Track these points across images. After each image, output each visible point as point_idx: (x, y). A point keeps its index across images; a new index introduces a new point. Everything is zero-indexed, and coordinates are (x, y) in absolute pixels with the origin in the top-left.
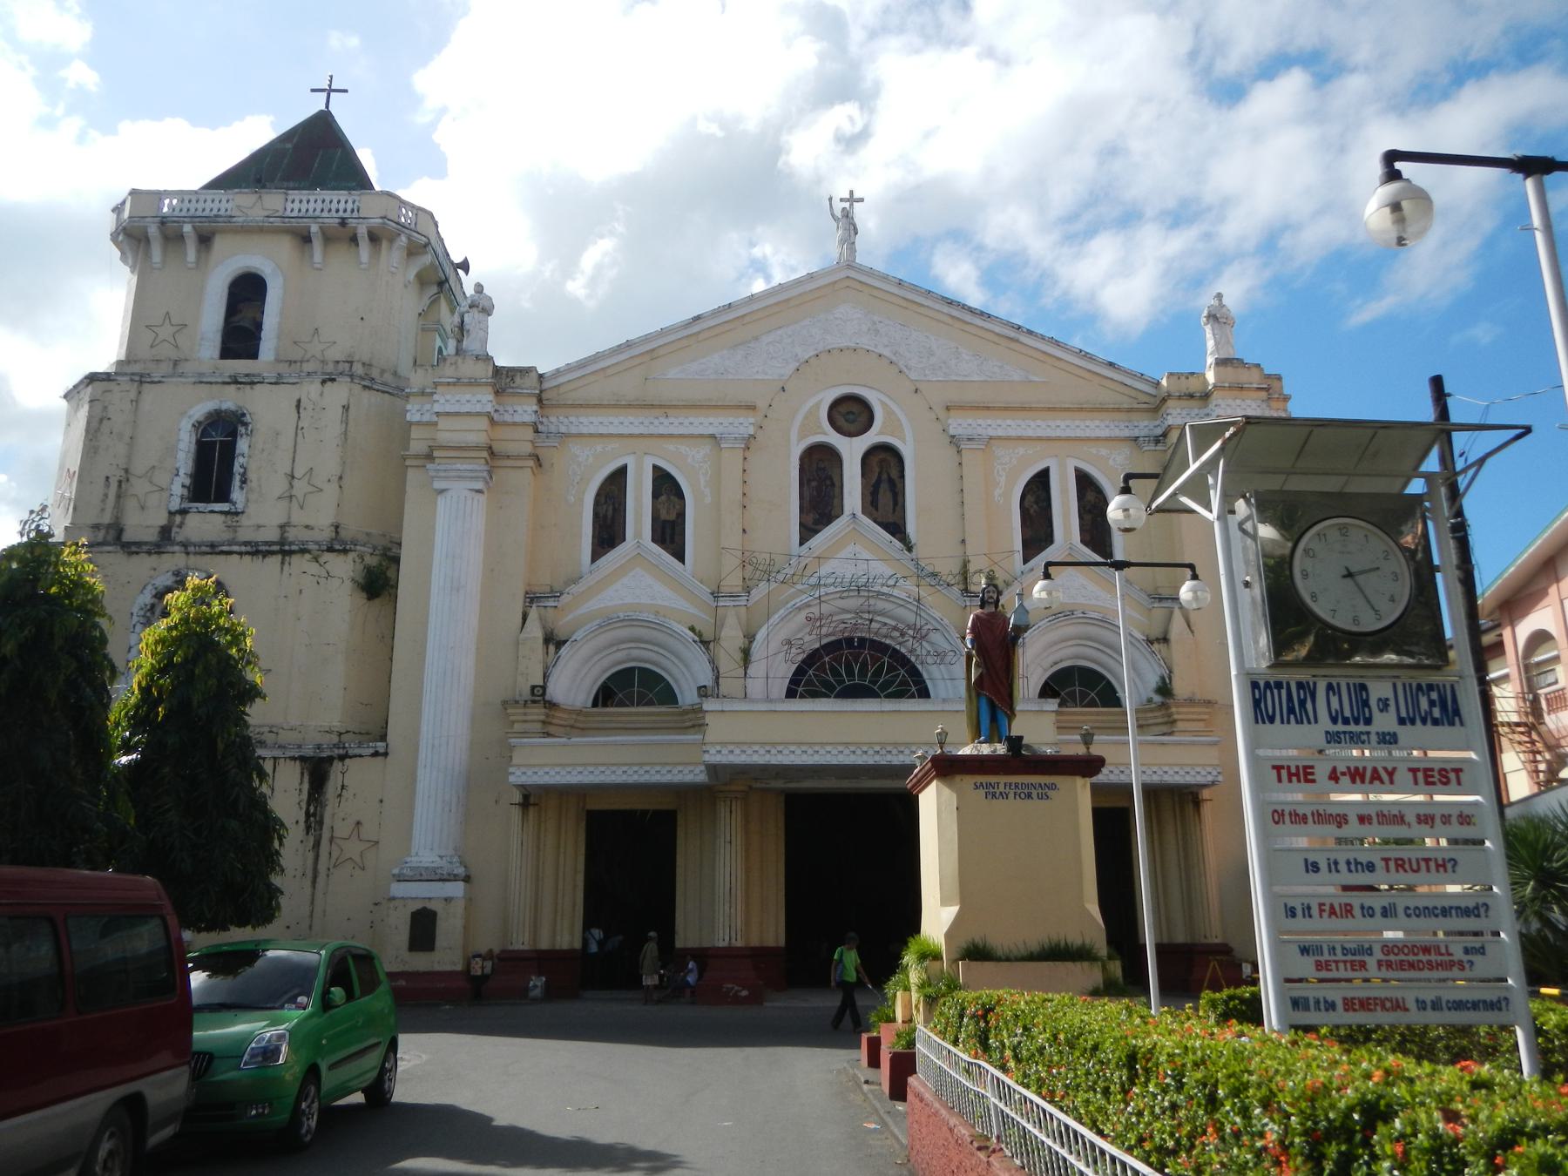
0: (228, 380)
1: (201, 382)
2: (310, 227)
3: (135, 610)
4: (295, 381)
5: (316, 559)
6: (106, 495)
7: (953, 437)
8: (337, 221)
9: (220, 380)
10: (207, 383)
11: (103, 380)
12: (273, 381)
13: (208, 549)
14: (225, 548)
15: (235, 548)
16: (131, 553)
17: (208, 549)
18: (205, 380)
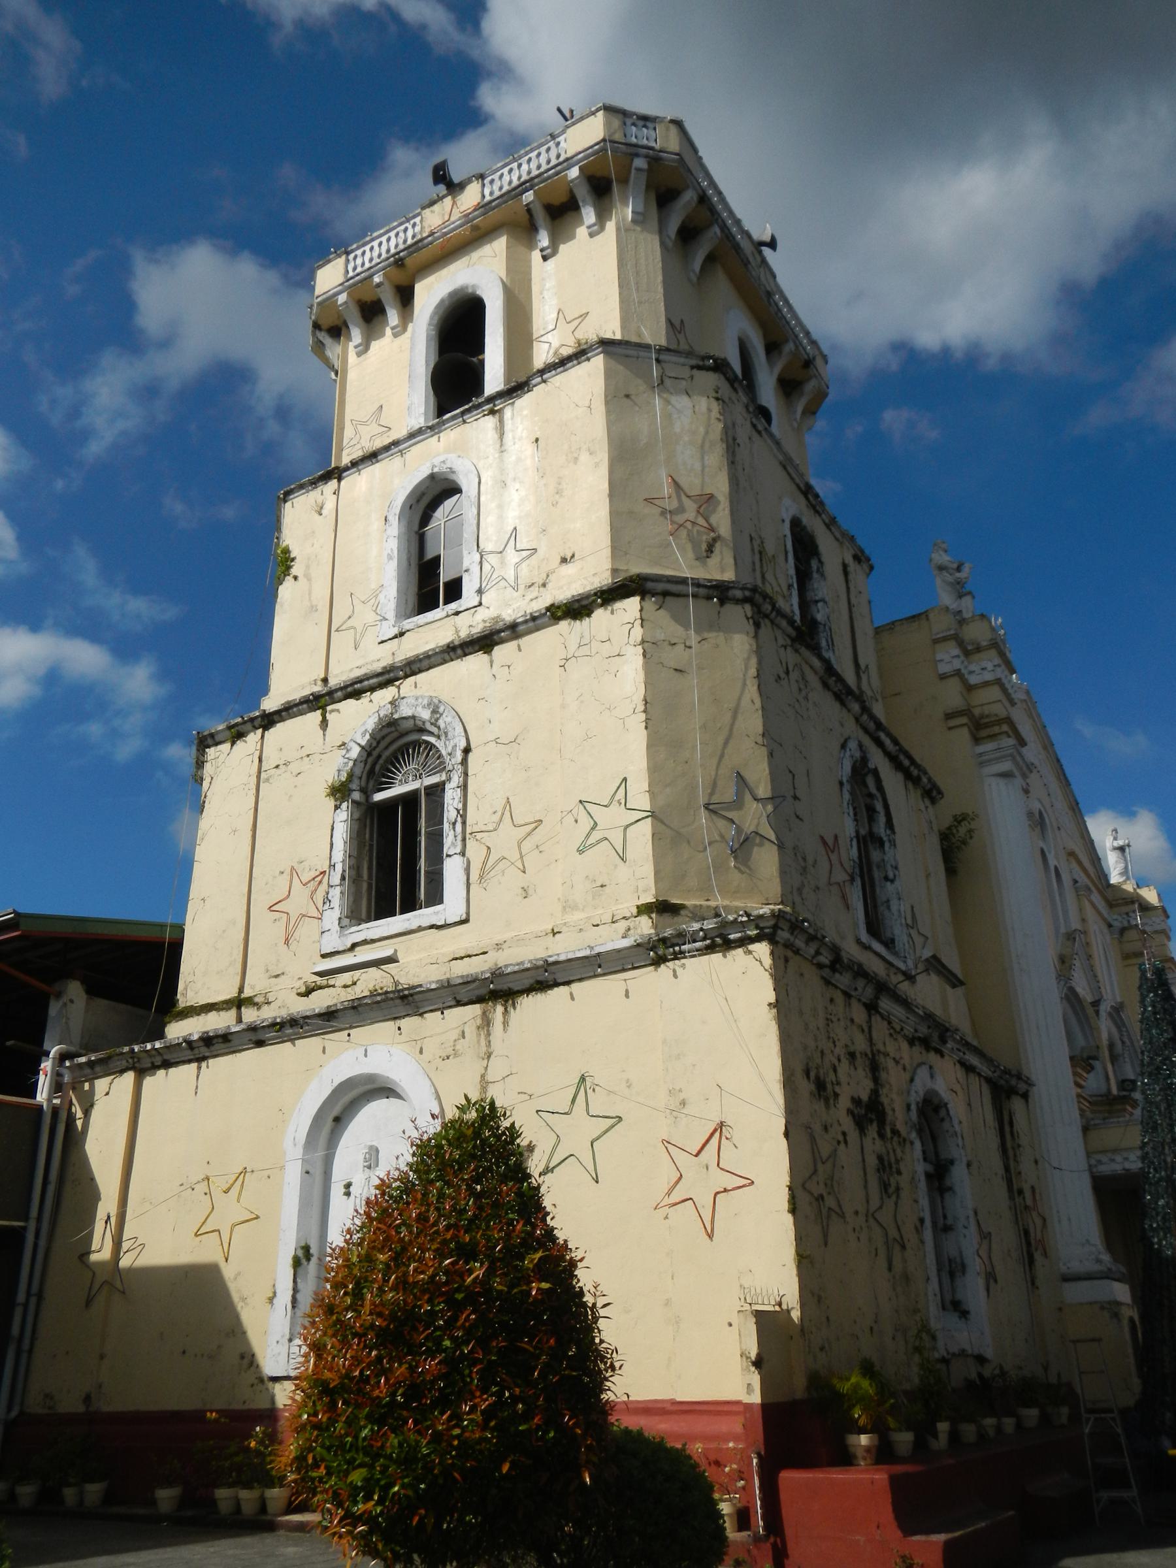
0: (803, 488)
1: (785, 468)
2: (787, 341)
3: (845, 780)
4: (838, 536)
5: (923, 797)
6: (754, 563)
7: (1076, 882)
8: (806, 357)
9: (798, 480)
10: (789, 474)
11: (728, 379)
12: (827, 521)
13: (872, 726)
14: (882, 736)
15: (887, 742)
16: (826, 685)
17: (872, 726)
18: (789, 468)
